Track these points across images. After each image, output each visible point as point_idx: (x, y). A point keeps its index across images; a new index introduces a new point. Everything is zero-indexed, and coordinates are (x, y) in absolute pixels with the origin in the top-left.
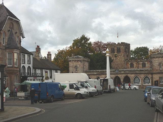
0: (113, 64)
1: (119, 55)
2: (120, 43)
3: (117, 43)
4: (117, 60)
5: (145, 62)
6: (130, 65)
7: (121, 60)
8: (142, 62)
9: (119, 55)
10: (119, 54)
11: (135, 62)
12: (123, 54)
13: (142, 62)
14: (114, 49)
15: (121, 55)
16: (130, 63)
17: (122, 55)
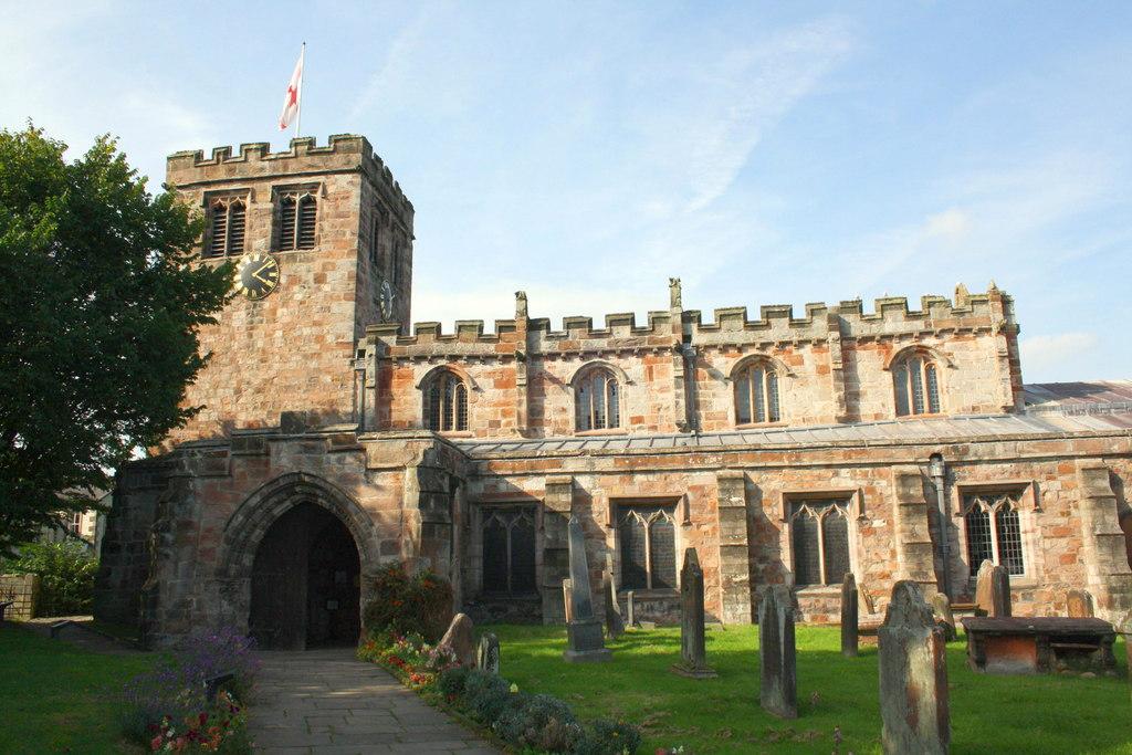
0: (216, 387)
1: (294, 280)
2: (322, 143)
3: (279, 146)
4: (259, 332)
5: (623, 354)
6: (418, 396)
7: (320, 339)
8: (577, 364)
9: (294, 280)
10: (293, 258)
11: (486, 359)
12: (346, 264)
13: (577, 364)
14: (240, 207)
15: (320, 279)
16: (422, 370)
17: (330, 276)
